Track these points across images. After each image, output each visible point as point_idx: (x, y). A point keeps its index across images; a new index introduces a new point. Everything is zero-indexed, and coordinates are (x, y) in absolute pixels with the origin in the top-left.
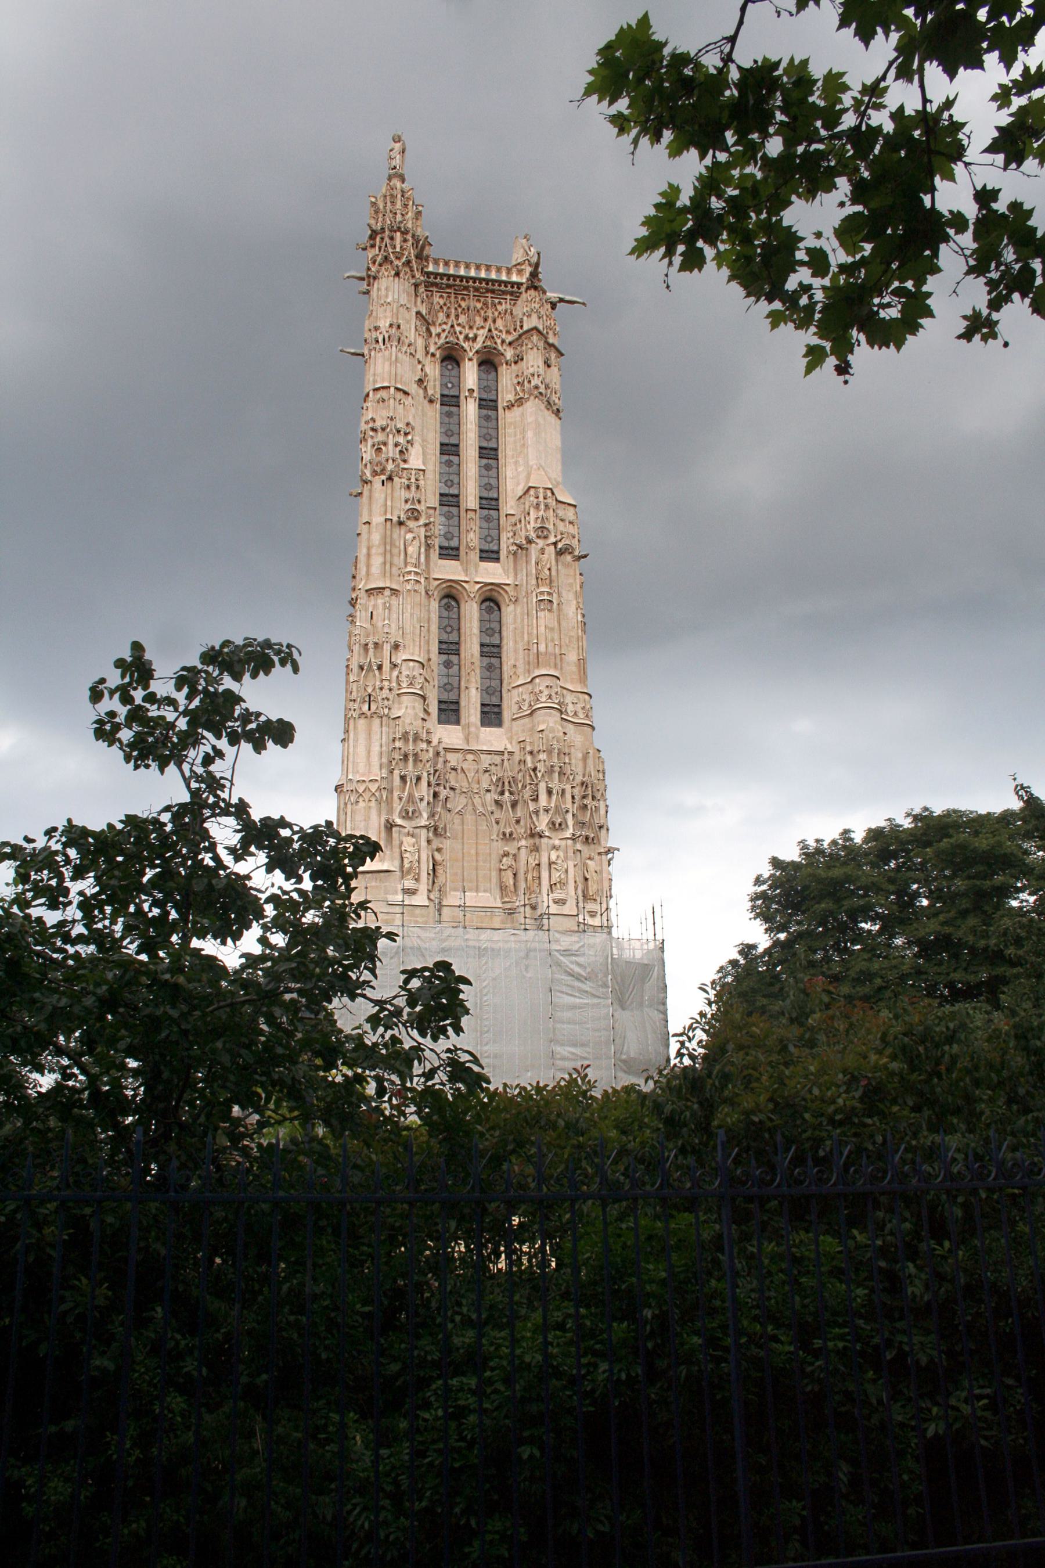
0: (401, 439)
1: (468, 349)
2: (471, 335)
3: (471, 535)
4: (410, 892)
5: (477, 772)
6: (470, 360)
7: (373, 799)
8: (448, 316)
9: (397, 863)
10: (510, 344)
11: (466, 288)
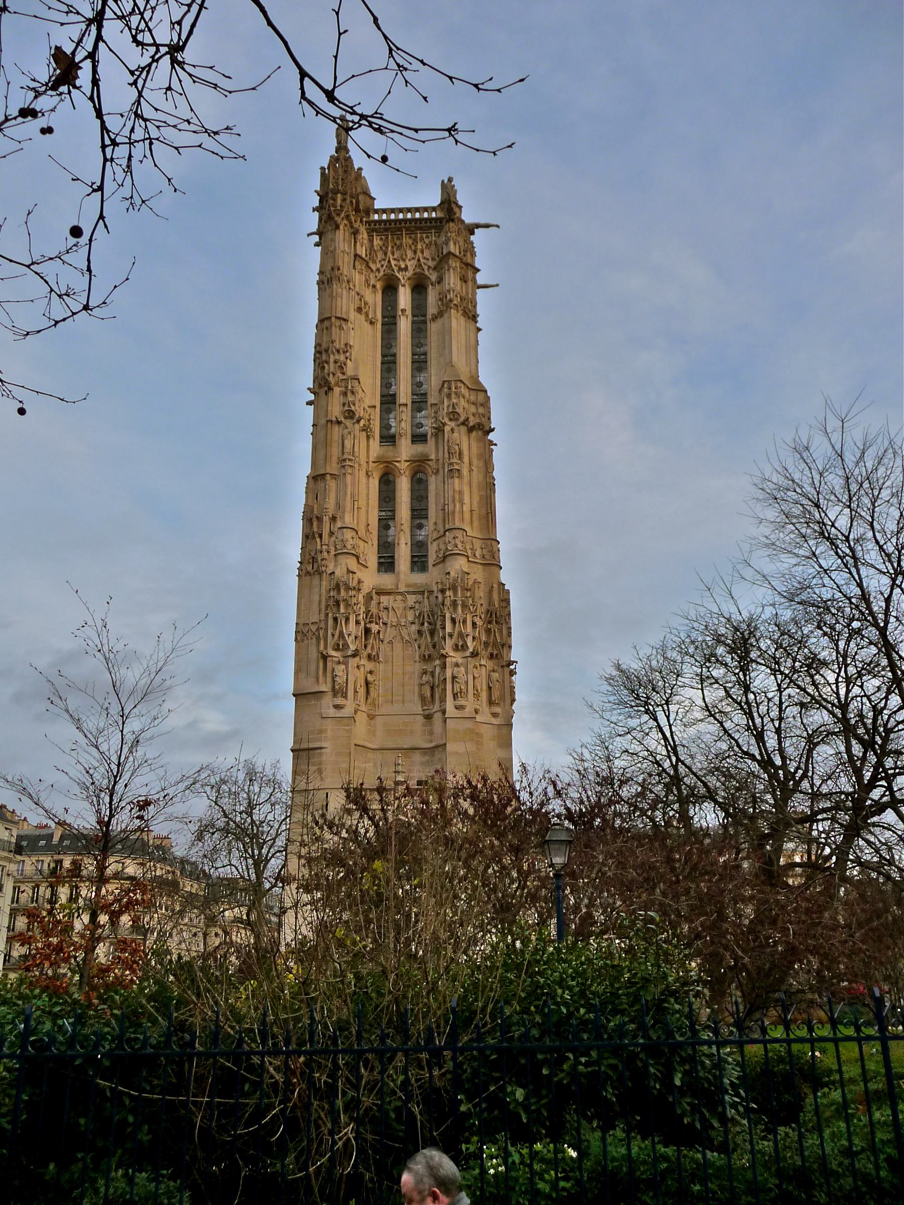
0: (342, 358)
2: (403, 266)
3: (403, 424)
5: (405, 608)
6: (404, 286)
7: (314, 638)
9: (329, 685)
10: (435, 268)
11: (400, 229)
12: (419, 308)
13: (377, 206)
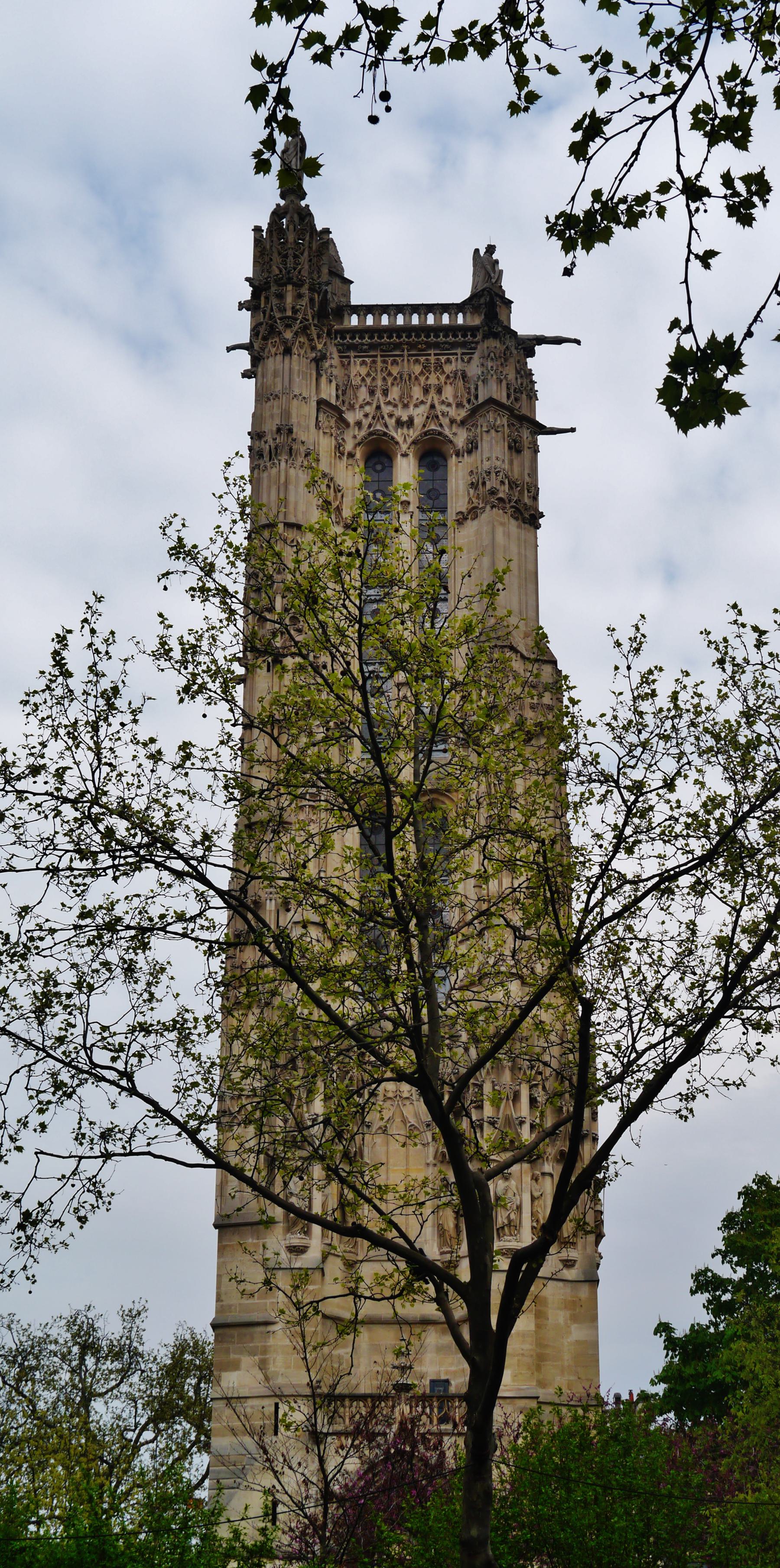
1: (400, 439)
2: (405, 418)
4: (298, 1250)
6: (405, 455)
8: (372, 392)
10: (463, 423)
11: (397, 346)
12: (433, 496)
13: (355, 301)
